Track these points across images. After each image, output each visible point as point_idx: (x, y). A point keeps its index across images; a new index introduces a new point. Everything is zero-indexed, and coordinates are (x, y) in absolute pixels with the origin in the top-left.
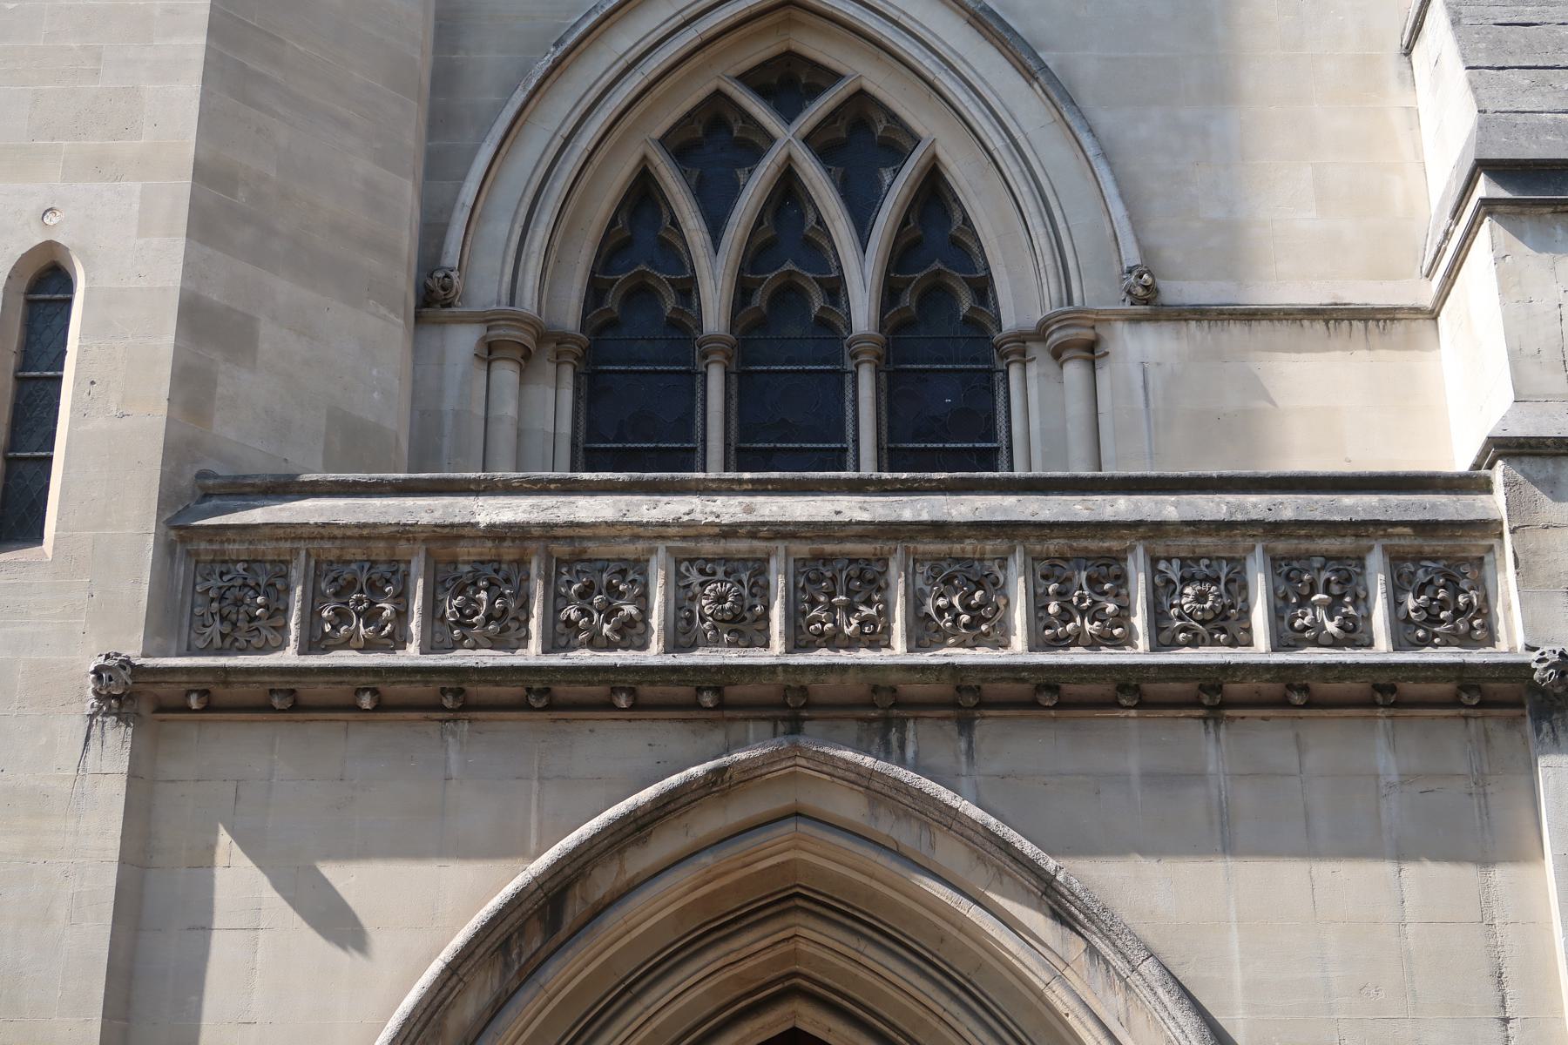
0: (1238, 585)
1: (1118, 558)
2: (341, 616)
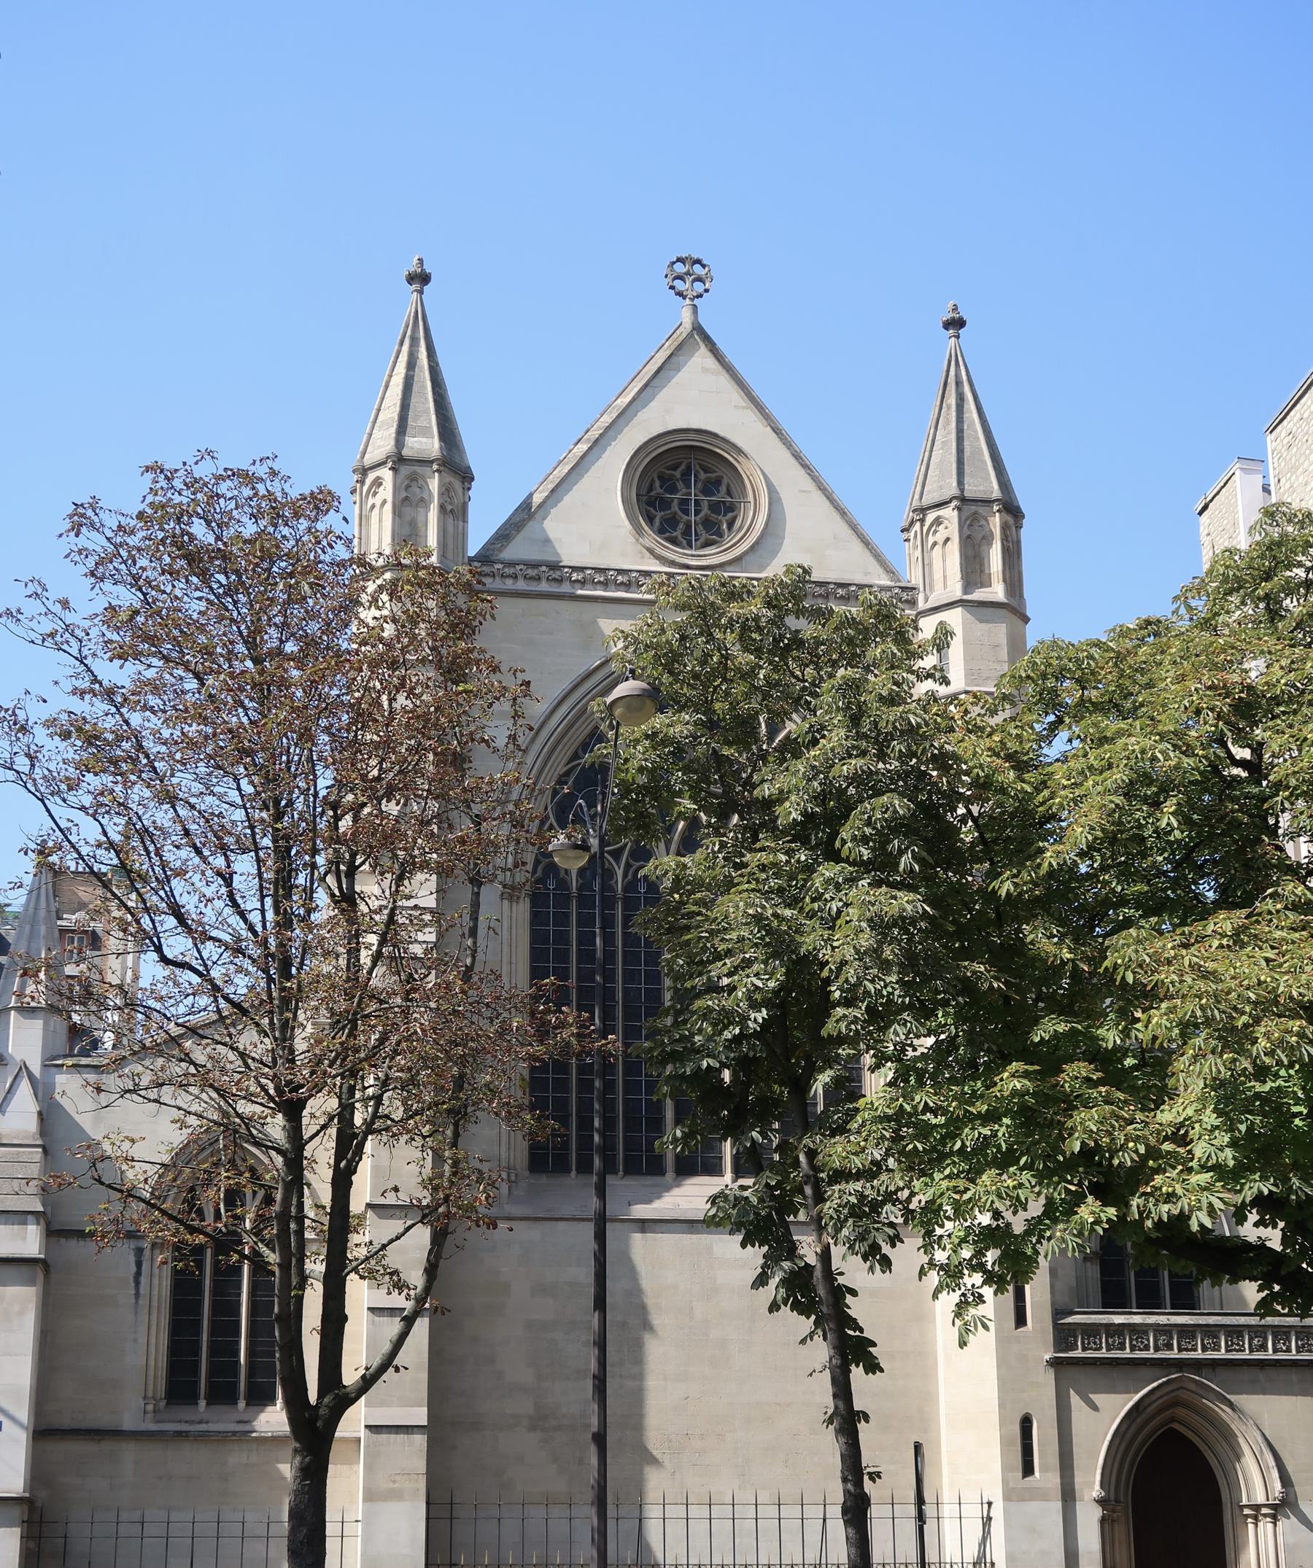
0: (1266, 1340)
1: (1241, 1332)
2: (1089, 1343)
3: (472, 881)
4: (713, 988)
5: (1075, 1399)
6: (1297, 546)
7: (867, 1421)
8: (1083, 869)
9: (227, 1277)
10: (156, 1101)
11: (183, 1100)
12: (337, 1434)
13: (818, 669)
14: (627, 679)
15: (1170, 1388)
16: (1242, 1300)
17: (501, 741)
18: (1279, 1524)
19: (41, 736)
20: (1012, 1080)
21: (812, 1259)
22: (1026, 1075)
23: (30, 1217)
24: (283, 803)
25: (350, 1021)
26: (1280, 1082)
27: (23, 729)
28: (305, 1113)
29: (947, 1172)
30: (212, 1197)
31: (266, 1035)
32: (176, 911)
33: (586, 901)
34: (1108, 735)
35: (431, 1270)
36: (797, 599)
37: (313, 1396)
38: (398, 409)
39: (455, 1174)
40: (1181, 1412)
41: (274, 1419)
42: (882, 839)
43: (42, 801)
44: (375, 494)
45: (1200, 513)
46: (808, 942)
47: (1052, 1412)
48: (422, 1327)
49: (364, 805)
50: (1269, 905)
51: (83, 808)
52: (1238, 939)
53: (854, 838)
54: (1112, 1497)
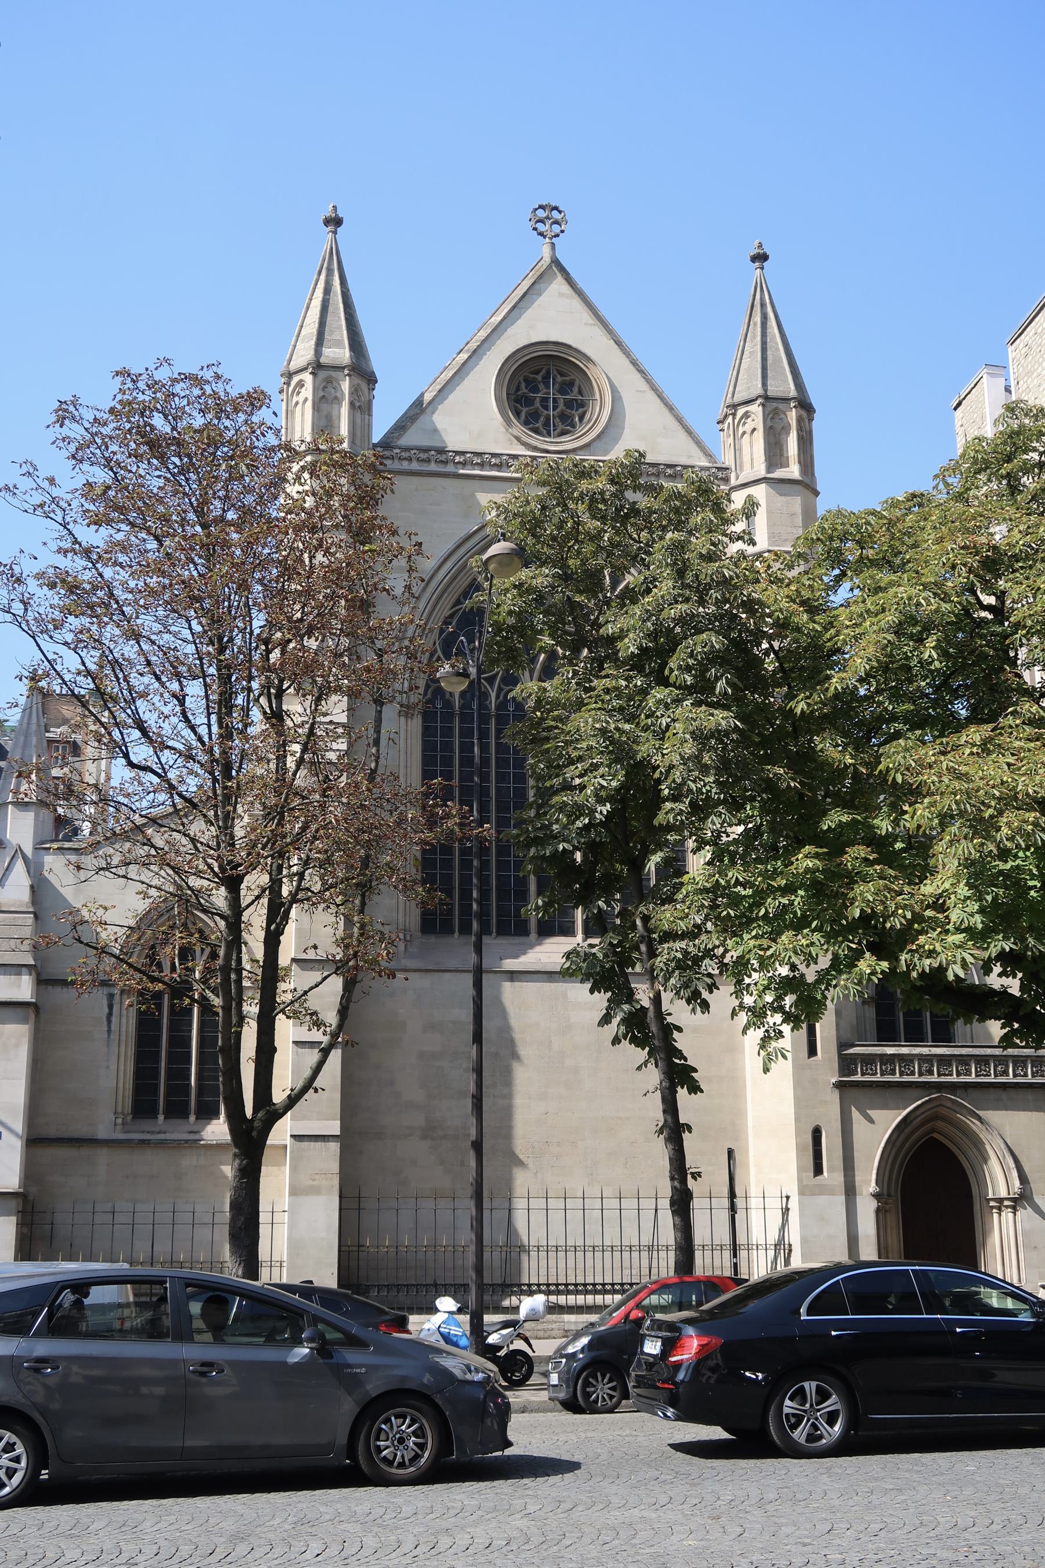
0: (1007, 1067)
3: (375, 701)
4: (567, 787)
5: (855, 1114)
6: (1032, 435)
7: (690, 1132)
8: (862, 692)
9: (181, 1017)
10: (124, 877)
11: (146, 876)
12: (268, 1142)
13: (651, 532)
14: (499, 541)
15: (931, 1105)
16: (988, 1035)
17: (399, 590)
18: (1018, 1213)
19: (32, 586)
20: (805, 860)
21: (646, 1003)
22: (817, 856)
23: (24, 969)
24: (225, 639)
25: (278, 813)
26: (1019, 862)
27: (19, 581)
28: (243, 886)
29: (754, 933)
30: (169, 953)
31: (212, 824)
32: (140, 725)
33: (466, 718)
34: (882, 585)
35: (343, 1012)
36: (635, 477)
37: (249, 1112)
38: (317, 325)
39: (362, 935)
40: (940, 1124)
41: (218, 1130)
42: (702, 668)
43: (33, 638)
44: (298, 393)
45: (955, 409)
46: (643, 750)
47: (837, 1125)
48: (335, 1057)
49: (290, 641)
50: (1010, 720)
51: (66, 644)
52: (985, 748)
53: (680, 668)
54: (885, 1192)
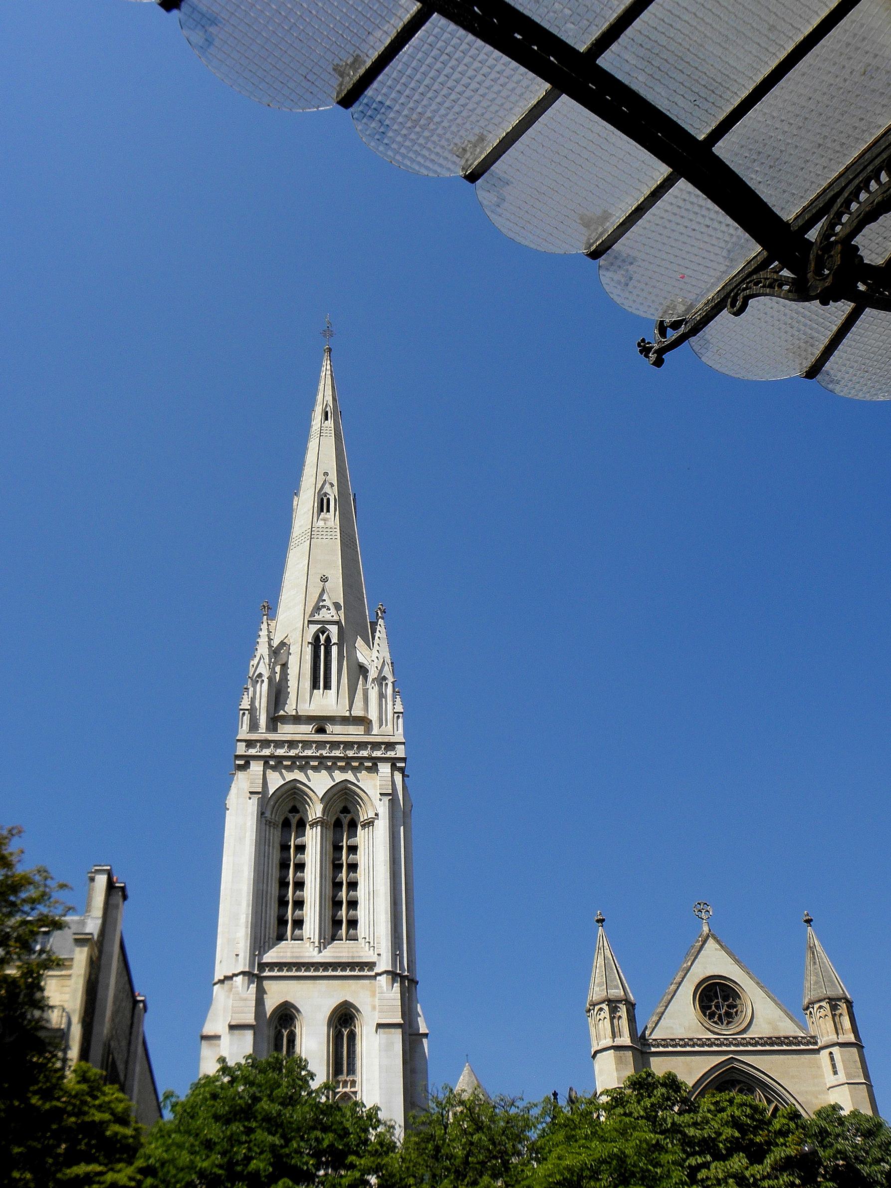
44: (600, 1014)
